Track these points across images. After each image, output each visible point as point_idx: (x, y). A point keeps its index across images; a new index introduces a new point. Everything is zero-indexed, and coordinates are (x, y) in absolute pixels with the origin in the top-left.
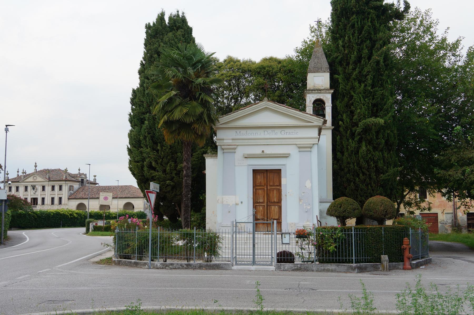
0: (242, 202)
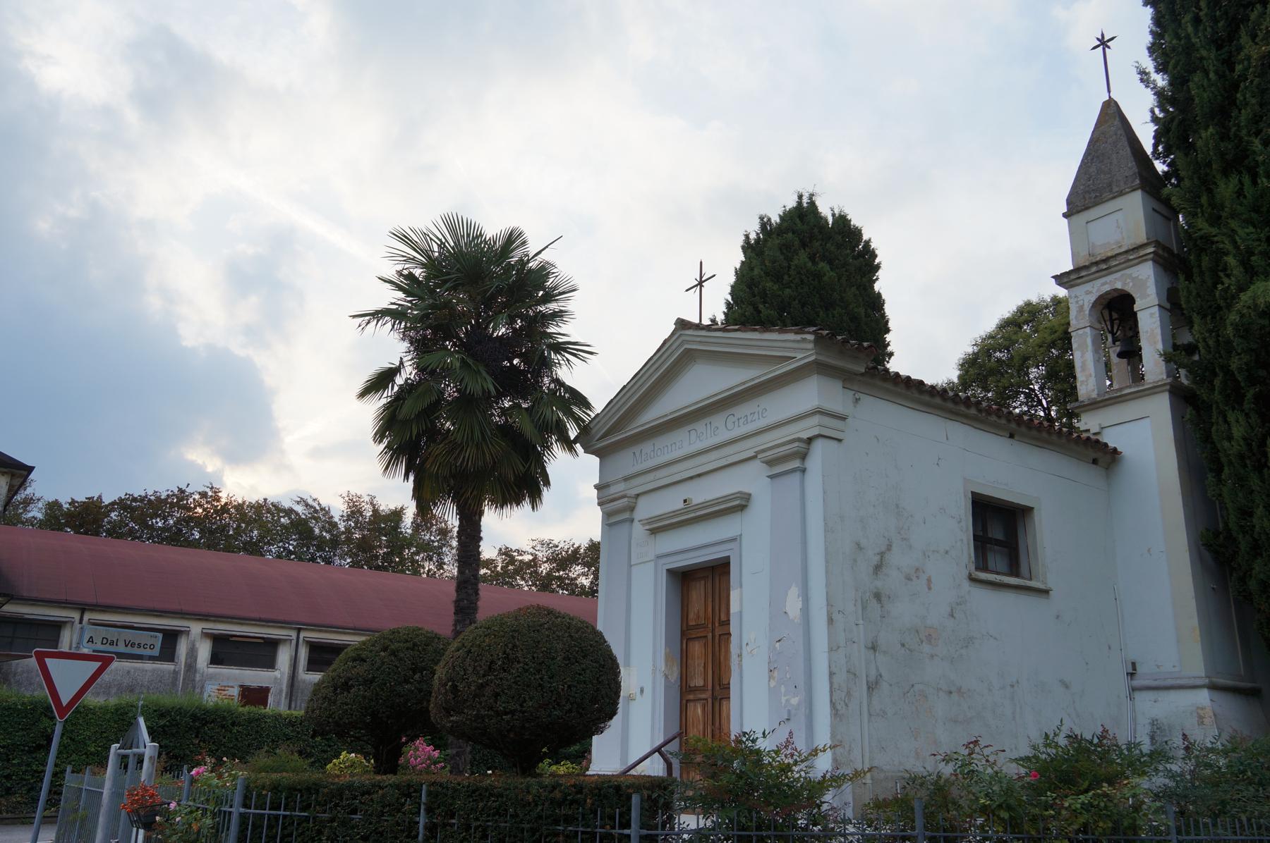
0: (642, 691)
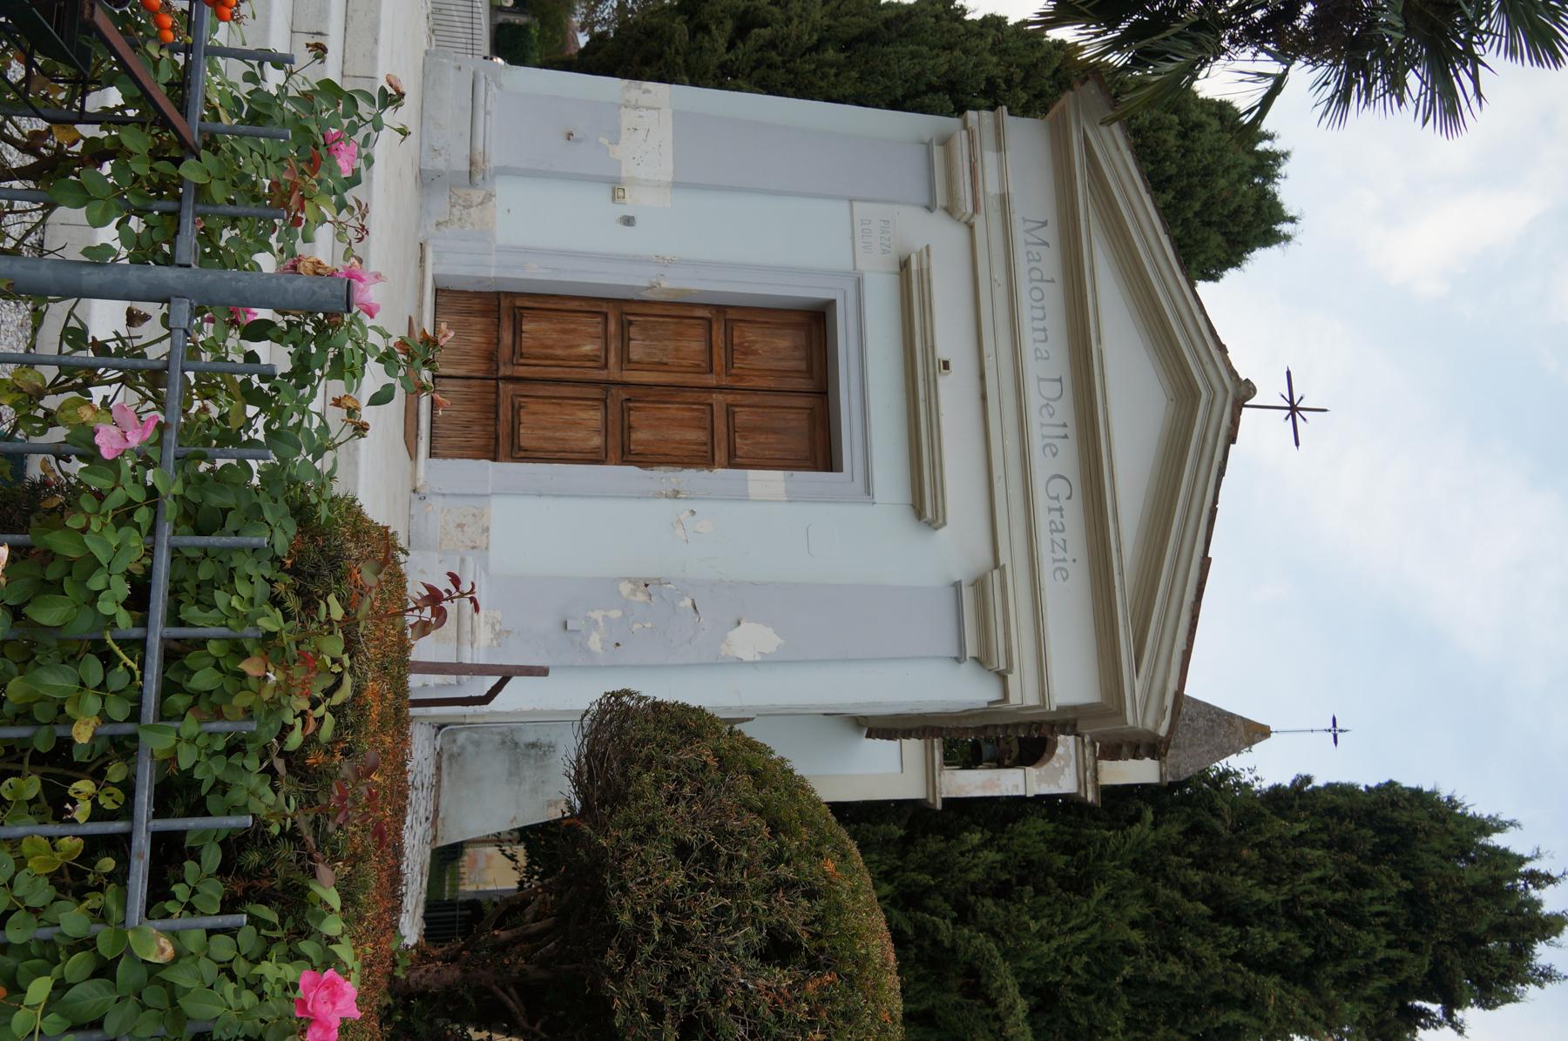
0: (628, 221)
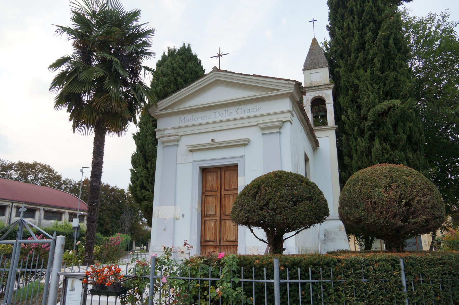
0: (183, 216)
